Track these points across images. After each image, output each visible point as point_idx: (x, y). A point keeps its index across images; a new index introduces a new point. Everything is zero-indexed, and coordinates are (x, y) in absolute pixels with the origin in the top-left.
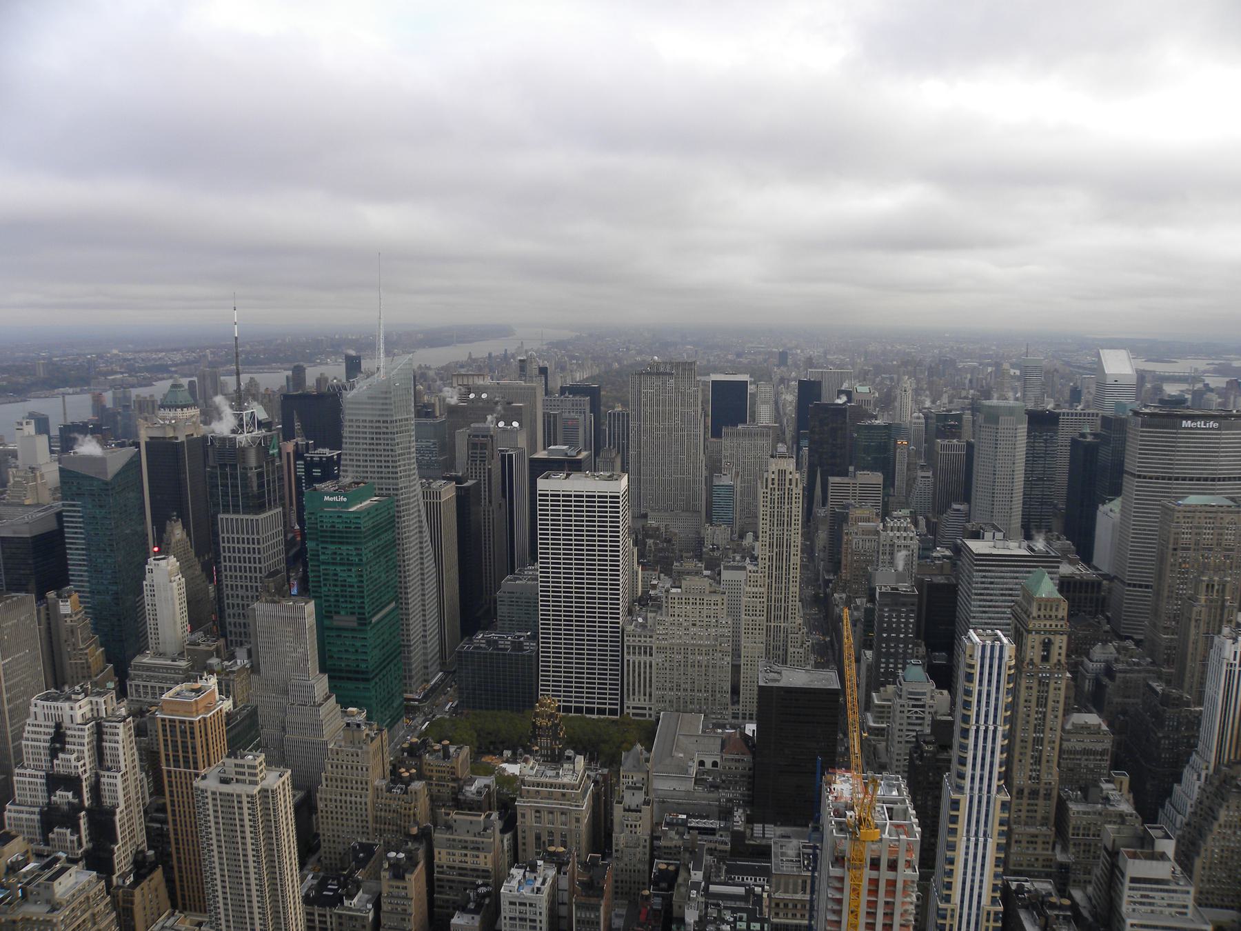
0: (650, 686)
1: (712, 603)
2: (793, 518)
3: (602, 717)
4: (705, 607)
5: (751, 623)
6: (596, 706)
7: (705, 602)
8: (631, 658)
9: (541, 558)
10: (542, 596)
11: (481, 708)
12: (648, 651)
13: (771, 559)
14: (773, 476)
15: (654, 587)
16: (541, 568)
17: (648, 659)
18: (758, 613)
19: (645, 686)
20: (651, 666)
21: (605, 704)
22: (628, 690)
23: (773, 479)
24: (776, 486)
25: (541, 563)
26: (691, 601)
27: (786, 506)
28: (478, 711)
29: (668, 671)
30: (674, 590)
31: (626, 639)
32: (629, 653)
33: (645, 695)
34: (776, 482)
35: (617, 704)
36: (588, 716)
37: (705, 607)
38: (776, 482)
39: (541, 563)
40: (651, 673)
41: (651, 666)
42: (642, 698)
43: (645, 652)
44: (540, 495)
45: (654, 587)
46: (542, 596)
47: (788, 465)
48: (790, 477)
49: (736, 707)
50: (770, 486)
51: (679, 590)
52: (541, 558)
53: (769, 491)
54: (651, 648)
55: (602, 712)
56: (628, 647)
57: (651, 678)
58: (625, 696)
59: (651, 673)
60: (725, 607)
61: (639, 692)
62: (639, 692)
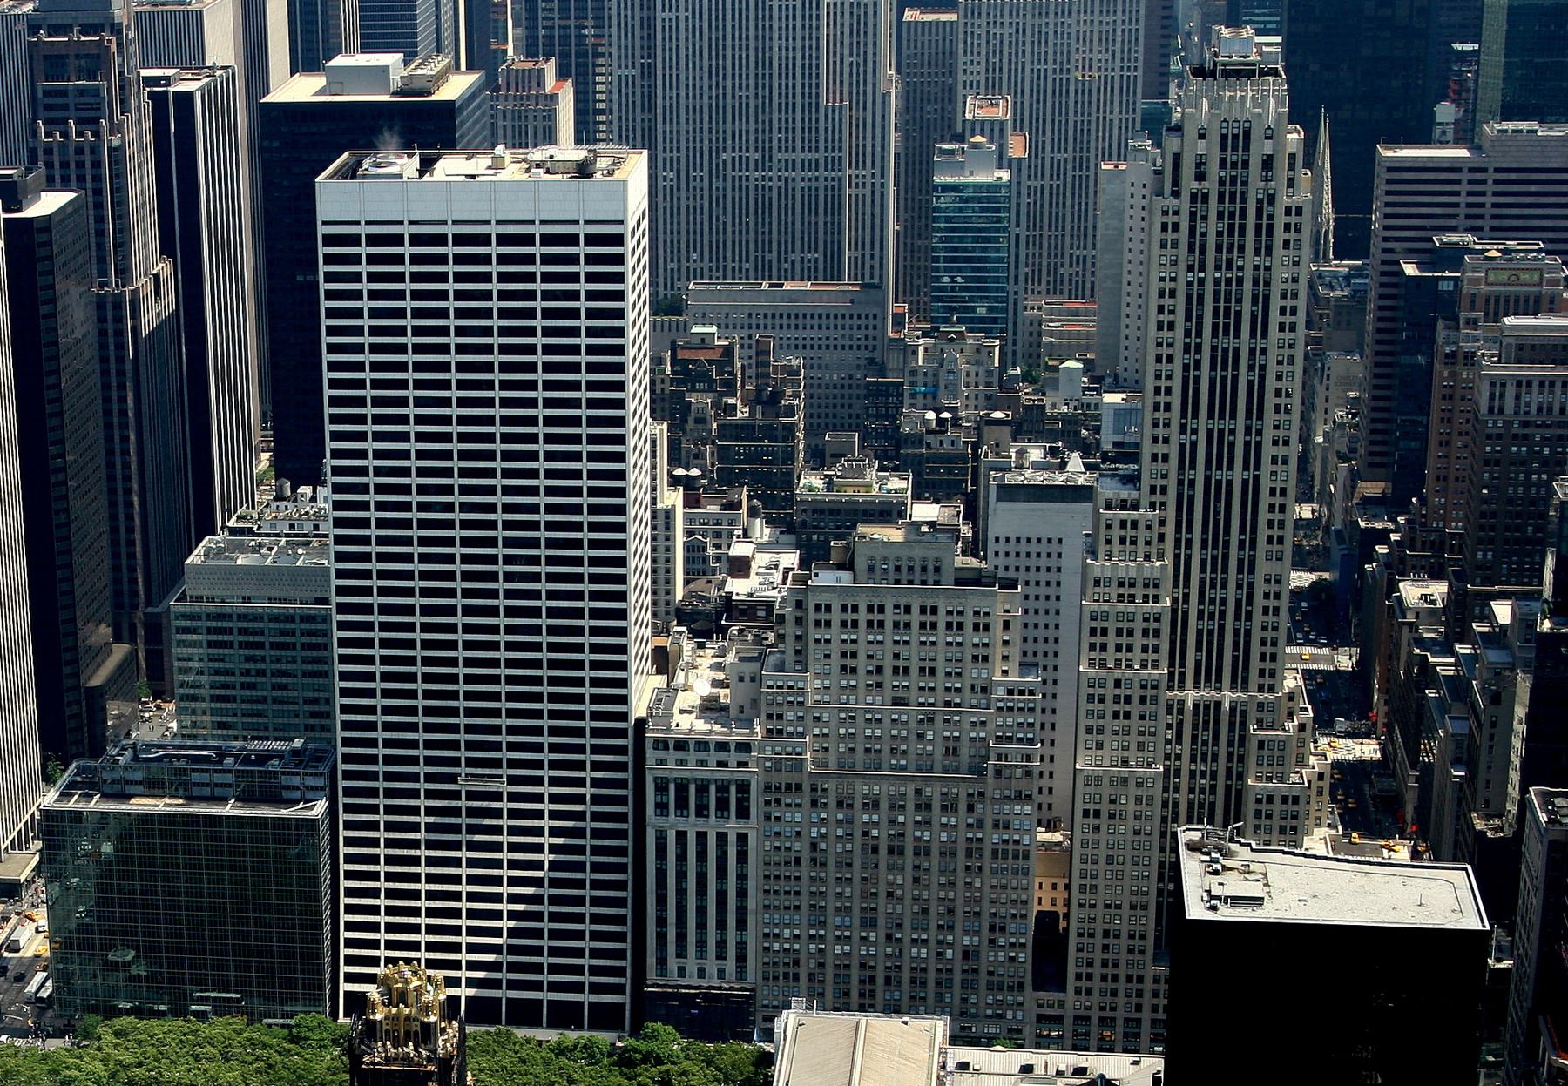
0: (742, 924)
1: (969, 621)
2: (1276, 303)
3: (572, 1035)
4: (942, 636)
5: (1110, 692)
6: (545, 996)
7: (942, 619)
8: (673, 823)
9: (337, 471)
10: (342, 608)
11: (138, 1012)
12: (730, 798)
13: (1187, 457)
14: (1201, 147)
15: (740, 567)
16: (337, 506)
17: (733, 826)
18: (1111, 656)
19: (722, 924)
20: (742, 857)
21: (578, 988)
22: (662, 938)
23: (1201, 163)
24: (1211, 186)
25: (337, 489)
26: (889, 617)
27: (1250, 260)
28: (123, 1022)
29: (805, 871)
30: (826, 578)
31: (651, 755)
32: (662, 807)
33: (721, 956)
34: (1213, 169)
35: (618, 989)
36: (521, 1033)
37: (942, 636)
38: (1213, 169)
39: (337, 489)
40: (742, 877)
41: (742, 857)
42: (712, 965)
43: (723, 805)
44: (330, 240)
45: (740, 567)
46: (342, 608)
47: (1263, 104)
48: (1268, 147)
49: (1051, 996)
50: (1189, 184)
51: (845, 577)
52: (337, 471)
53: (1185, 204)
54: (743, 787)
55: (564, 1016)
56: (662, 786)
57: (742, 893)
58: (651, 961)
59: (742, 877)
60: (1015, 634)
61: (702, 944)
62: (702, 944)
